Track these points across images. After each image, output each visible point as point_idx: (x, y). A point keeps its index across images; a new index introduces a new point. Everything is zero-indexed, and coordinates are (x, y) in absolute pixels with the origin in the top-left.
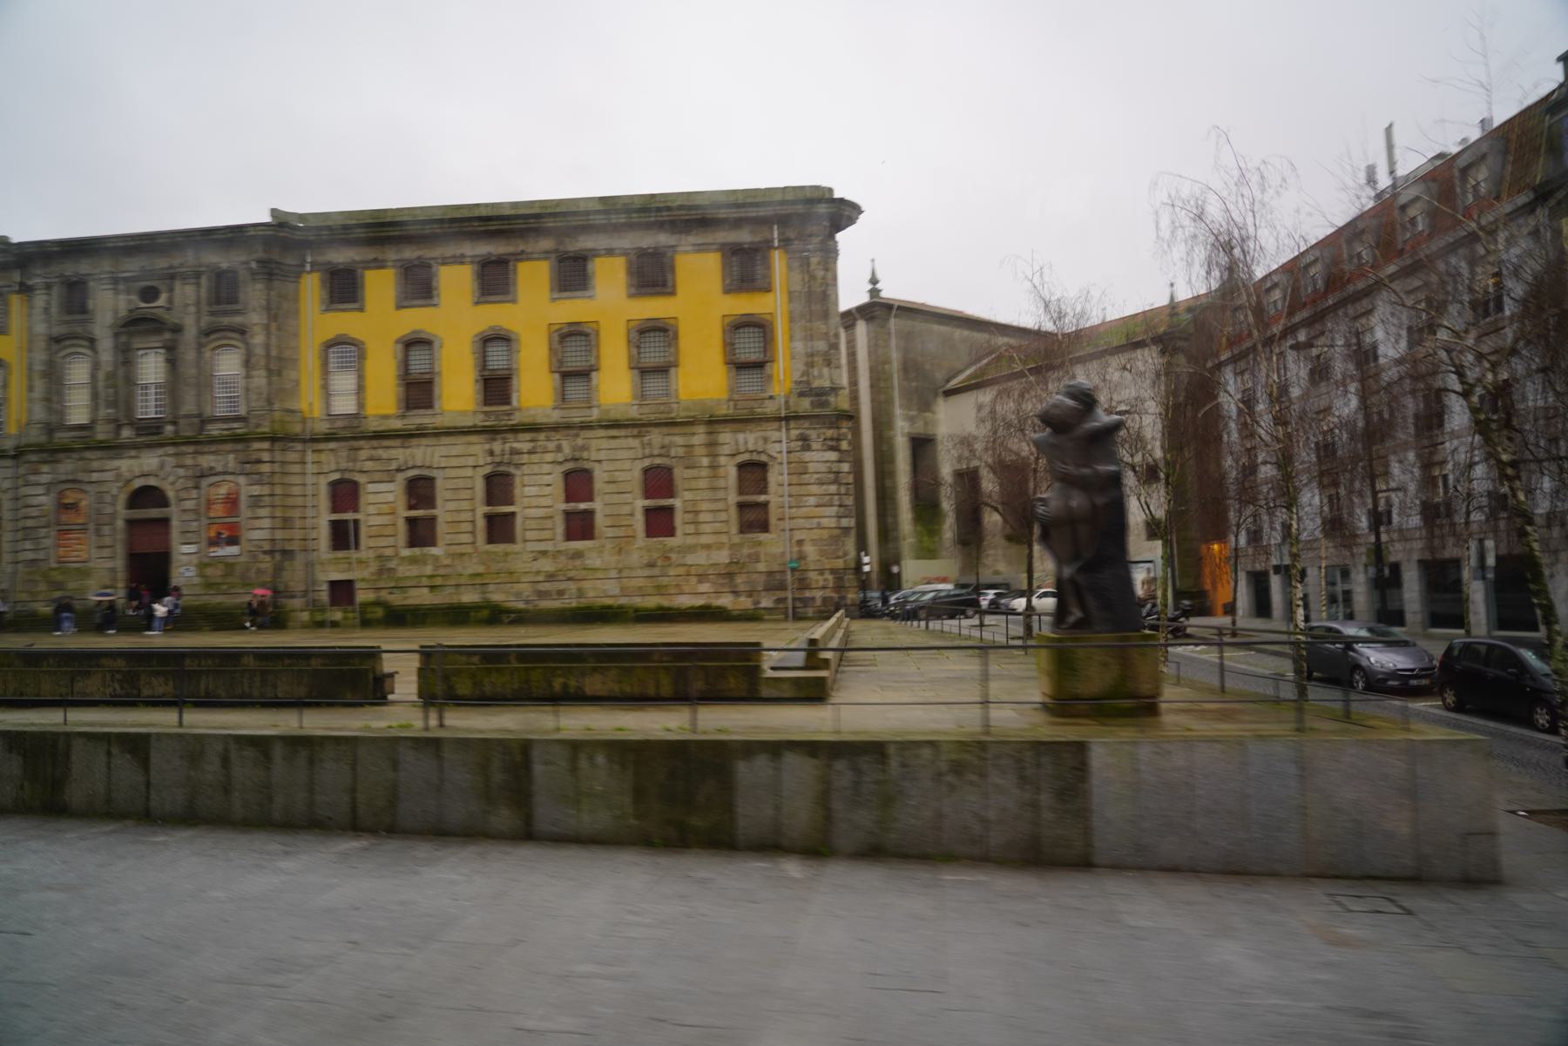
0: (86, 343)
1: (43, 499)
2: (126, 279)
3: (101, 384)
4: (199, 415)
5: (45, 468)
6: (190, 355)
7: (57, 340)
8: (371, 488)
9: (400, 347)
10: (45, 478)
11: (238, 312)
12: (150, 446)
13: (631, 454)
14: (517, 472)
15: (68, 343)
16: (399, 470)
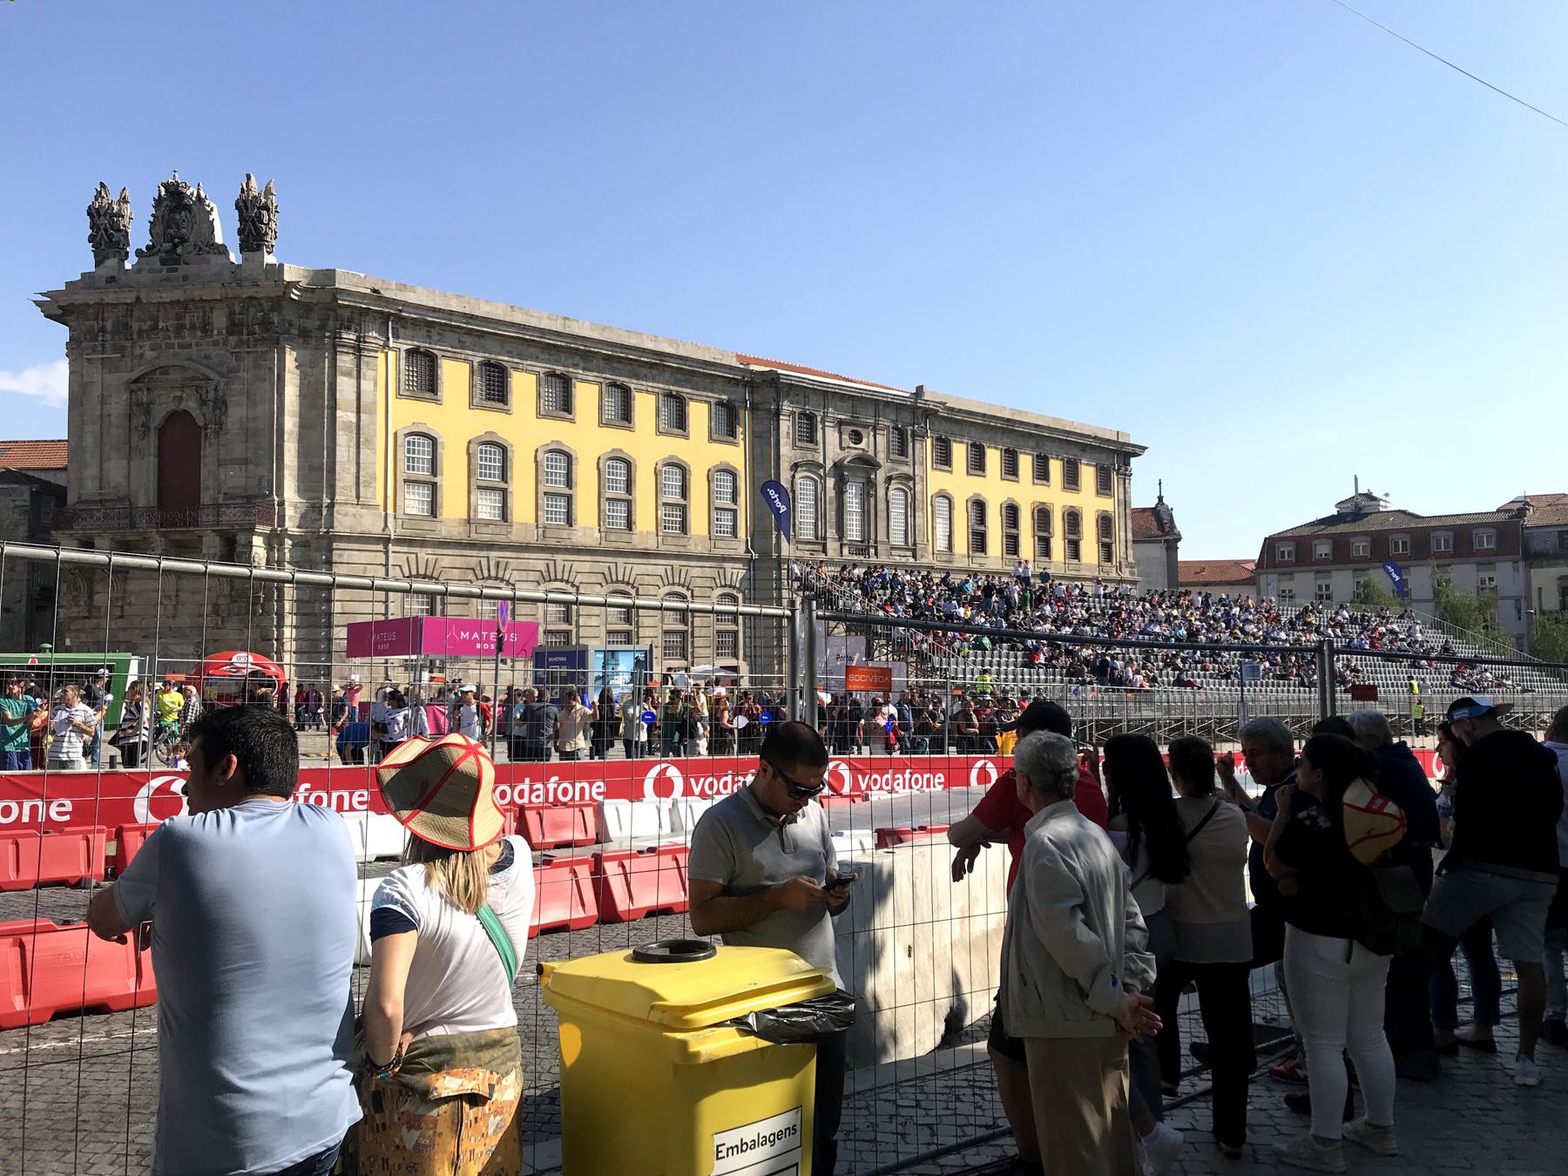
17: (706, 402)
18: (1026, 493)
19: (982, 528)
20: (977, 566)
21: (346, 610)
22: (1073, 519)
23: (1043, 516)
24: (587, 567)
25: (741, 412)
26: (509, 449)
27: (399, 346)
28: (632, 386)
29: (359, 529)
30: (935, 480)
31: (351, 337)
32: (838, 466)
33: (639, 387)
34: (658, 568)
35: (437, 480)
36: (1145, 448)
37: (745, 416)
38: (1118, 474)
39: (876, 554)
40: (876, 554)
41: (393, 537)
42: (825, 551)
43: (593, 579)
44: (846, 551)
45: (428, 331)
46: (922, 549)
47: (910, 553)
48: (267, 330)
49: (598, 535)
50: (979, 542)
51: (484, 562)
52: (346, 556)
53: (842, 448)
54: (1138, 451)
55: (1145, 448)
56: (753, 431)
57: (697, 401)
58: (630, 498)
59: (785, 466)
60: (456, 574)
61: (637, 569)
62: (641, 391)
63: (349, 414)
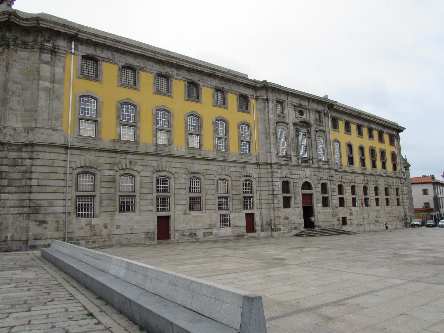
0: (286, 125)
1: (279, 183)
2: (295, 106)
3: (290, 142)
4: (317, 159)
5: (279, 171)
6: (313, 137)
7: (277, 123)
8: (346, 187)
9: (347, 145)
10: (279, 175)
11: (322, 126)
12: (307, 167)
13: (383, 184)
14: (368, 186)
15: (280, 124)
16: (350, 183)
17: (235, 94)
18: (367, 143)
19: (352, 155)
20: (351, 170)
21: (41, 184)
22: (383, 153)
23: (373, 152)
24: (178, 165)
25: (251, 100)
26: (138, 107)
27: (78, 53)
28: (200, 84)
29: (50, 141)
30: (333, 135)
31: (50, 45)
32: (295, 124)
33: (203, 84)
34: (215, 167)
35: (99, 119)
36: (405, 128)
37: (253, 104)
38: (396, 138)
39: (313, 163)
40: (313, 163)
41: (69, 146)
42: (291, 161)
43: (182, 171)
44: (300, 161)
45: (94, 48)
46: (331, 162)
47: (325, 163)
48: (3, 41)
49: (184, 150)
50: (351, 161)
51: (123, 161)
52: (41, 155)
53: (296, 117)
54: (403, 129)
55: (405, 128)
56: (257, 108)
57: (231, 93)
58: (200, 133)
59: (272, 123)
60: (108, 166)
61: (203, 167)
62: (204, 86)
63: (47, 83)
